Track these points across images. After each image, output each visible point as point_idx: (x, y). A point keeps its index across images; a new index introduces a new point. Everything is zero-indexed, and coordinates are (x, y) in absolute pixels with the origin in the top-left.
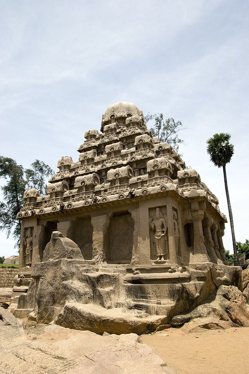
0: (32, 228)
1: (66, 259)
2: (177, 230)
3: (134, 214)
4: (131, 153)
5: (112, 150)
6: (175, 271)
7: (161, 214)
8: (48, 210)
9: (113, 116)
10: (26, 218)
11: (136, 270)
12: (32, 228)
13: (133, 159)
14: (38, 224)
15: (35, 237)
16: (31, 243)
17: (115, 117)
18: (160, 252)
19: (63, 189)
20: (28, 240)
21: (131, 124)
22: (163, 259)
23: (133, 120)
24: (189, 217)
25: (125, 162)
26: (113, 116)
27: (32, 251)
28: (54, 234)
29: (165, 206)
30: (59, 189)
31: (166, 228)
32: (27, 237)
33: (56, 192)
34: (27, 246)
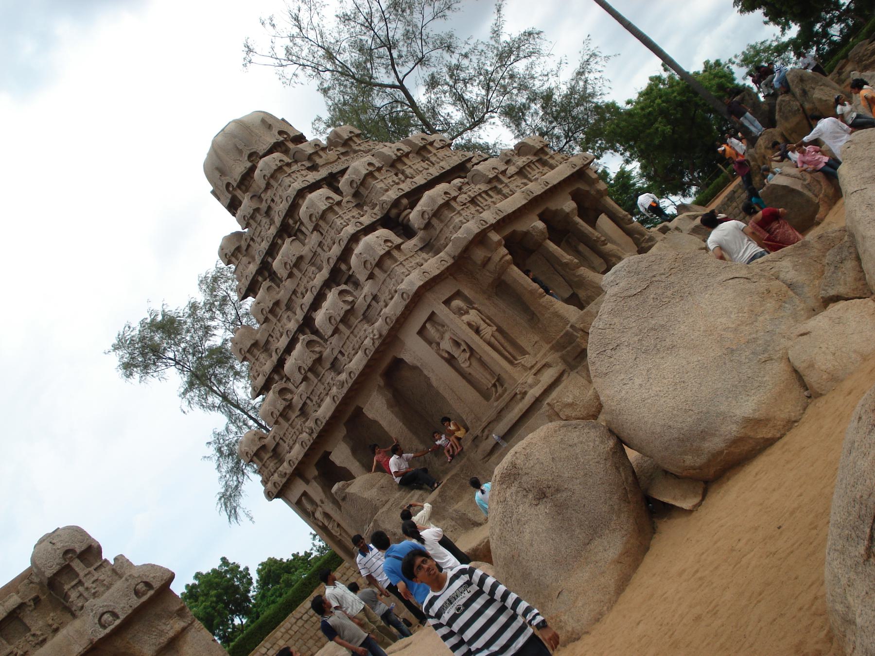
0: (305, 494)
1: (381, 511)
2: (483, 326)
3: (407, 358)
4: (319, 245)
5: (288, 267)
6: (525, 393)
7: (440, 328)
8: (296, 453)
9: (228, 185)
10: (281, 489)
11: (483, 431)
12: (305, 494)
13: (331, 260)
14: (307, 482)
15: (323, 502)
16: (326, 515)
17: (235, 184)
18: (486, 380)
19: (284, 399)
20: (318, 515)
21: (272, 182)
22: (500, 390)
23: (264, 172)
24: (487, 277)
25: (325, 273)
26: (228, 185)
27: (339, 525)
28: (336, 493)
29: (433, 313)
30: (281, 405)
31: (463, 343)
32: (313, 514)
33: (281, 415)
34: (326, 524)
